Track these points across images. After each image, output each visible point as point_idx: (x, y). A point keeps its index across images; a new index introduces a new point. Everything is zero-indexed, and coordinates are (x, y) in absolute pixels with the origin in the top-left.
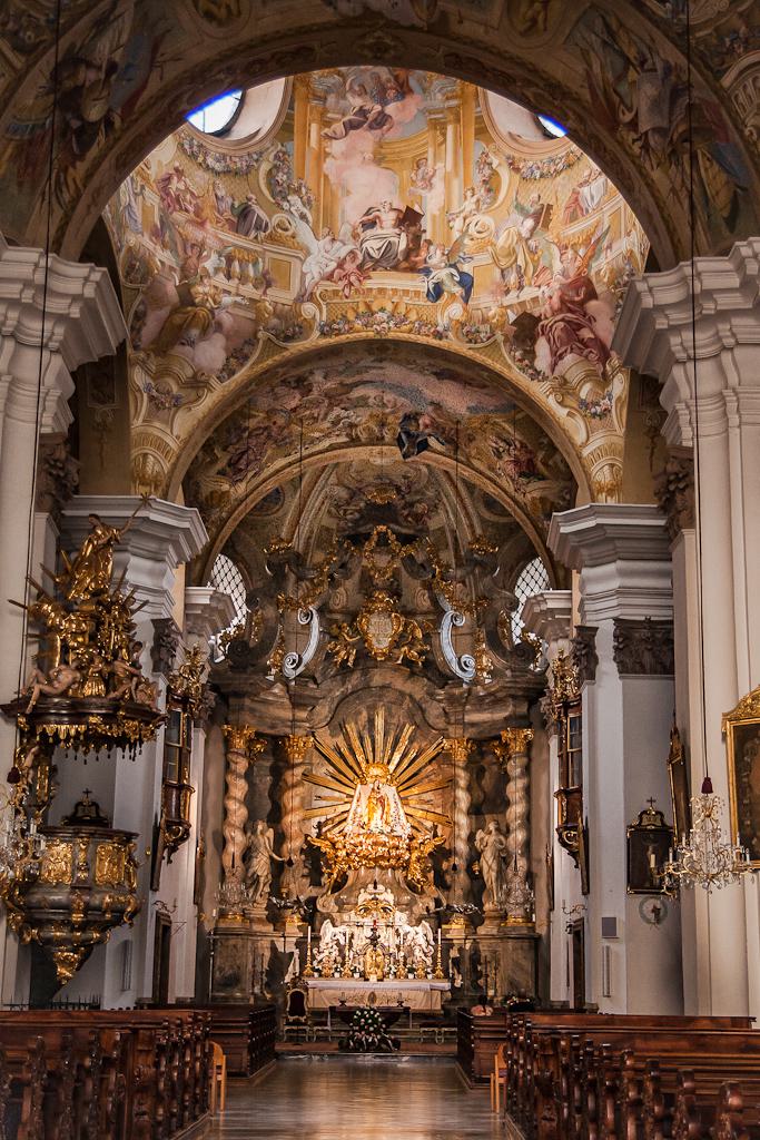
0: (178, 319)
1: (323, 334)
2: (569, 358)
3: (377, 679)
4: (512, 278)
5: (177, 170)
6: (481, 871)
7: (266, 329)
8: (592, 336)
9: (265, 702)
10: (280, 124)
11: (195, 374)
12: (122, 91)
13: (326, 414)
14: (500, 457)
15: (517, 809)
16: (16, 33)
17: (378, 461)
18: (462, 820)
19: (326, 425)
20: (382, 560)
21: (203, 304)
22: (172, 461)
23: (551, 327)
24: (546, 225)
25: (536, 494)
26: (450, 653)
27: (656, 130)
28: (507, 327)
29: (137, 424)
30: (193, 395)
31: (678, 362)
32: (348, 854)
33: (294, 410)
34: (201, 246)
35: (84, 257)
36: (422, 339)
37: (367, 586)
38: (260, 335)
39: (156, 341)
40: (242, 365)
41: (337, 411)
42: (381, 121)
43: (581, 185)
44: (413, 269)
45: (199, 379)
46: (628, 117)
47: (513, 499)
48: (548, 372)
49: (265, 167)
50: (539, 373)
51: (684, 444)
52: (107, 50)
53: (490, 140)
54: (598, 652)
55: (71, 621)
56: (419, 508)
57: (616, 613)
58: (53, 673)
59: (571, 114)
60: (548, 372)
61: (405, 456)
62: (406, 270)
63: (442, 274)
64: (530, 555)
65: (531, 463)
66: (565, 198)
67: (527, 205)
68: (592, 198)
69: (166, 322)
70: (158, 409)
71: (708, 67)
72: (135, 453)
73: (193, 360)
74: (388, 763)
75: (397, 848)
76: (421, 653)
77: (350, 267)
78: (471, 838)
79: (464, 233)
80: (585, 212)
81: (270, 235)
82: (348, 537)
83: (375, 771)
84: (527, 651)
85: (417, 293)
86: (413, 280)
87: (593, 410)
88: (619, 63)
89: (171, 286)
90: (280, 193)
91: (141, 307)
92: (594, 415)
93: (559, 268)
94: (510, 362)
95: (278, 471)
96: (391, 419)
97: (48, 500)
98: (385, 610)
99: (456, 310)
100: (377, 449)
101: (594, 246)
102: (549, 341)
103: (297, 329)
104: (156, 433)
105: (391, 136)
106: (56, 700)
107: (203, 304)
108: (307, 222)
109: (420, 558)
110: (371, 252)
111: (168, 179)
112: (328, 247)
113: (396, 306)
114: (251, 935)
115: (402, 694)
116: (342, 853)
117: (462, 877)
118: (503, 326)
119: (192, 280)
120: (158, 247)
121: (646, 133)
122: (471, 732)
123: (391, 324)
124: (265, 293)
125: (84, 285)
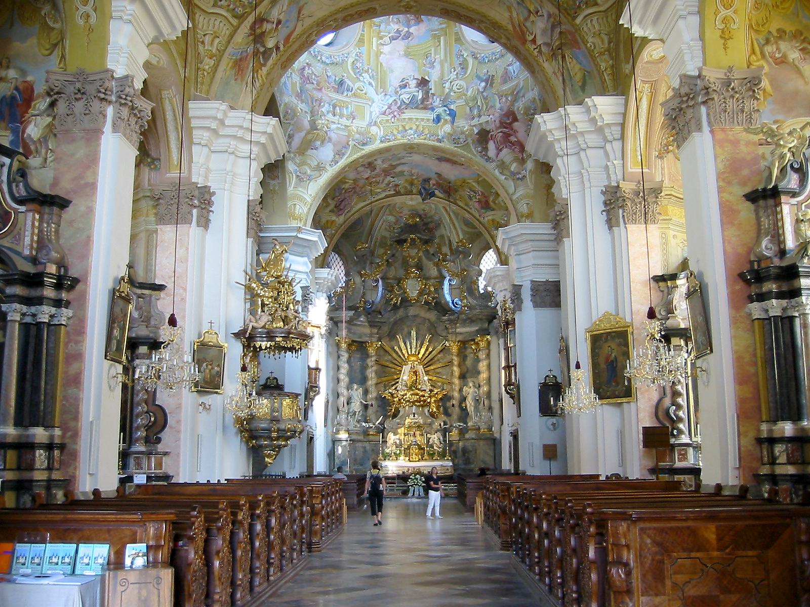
0: (309, 137)
1: (382, 142)
2: (505, 151)
3: (412, 311)
4: (476, 112)
5: (307, 64)
6: (466, 407)
7: (353, 140)
9: (356, 325)
11: (319, 163)
12: (284, 32)
13: (383, 180)
14: (470, 198)
15: (484, 376)
16: (234, 9)
17: (410, 203)
19: (383, 185)
20: (413, 252)
21: (321, 130)
22: (308, 207)
24: (491, 85)
25: (490, 218)
26: (448, 298)
27: (545, 44)
28: (474, 136)
29: (290, 189)
30: (318, 175)
31: (559, 156)
32: (399, 400)
33: (367, 179)
34: (320, 101)
35: (267, 113)
36: (431, 143)
37: (406, 265)
38: (350, 143)
41: (389, 178)
42: (408, 35)
43: (508, 66)
44: (425, 108)
46: (531, 38)
47: (478, 220)
48: (494, 158)
49: (350, 60)
50: (490, 158)
51: (563, 197)
52: (276, 15)
53: (462, 44)
54: (523, 297)
55: (265, 291)
56: (431, 225)
57: (530, 278)
58: (258, 317)
59: (503, 36)
60: (494, 158)
61: (423, 200)
62: (422, 109)
63: (440, 110)
64: (487, 248)
65: (487, 203)
66: (501, 72)
67: (482, 75)
68: (514, 72)
71: (568, 14)
72: (290, 204)
75: (424, 396)
76: (433, 298)
77: (394, 108)
78: (461, 390)
79: (451, 90)
80: (511, 79)
81: (354, 93)
82: (396, 241)
83: (413, 358)
84: (488, 296)
85: (428, 120)
86: (426, 113)
87: (517, 176)
88: (526, 13)
89: (306, 122)
90: (358, 72)
91: (292, 132)
92: (519, 178)
93: (499, 105)
95: (360, 209)
96: (416, 182)
97: (252, 232)
98: (414, 277)
99: (448, 128)
100: (409, 197)
101: (516, 95)
105: (412, 43)
106: (260, 330)
108: (372, 86)
109: (432, 251)
110: (404, 100)
111: (304, 69)
112: (383, 98)
113: (418, 126)
117: (457, 409)
118: (471, 135)
119: (316, 117)
120: (299, 102)
121: (540, 45)
122: (460, 338)
123: (416, 136)
124: (352, 122)
125: (267, 127)
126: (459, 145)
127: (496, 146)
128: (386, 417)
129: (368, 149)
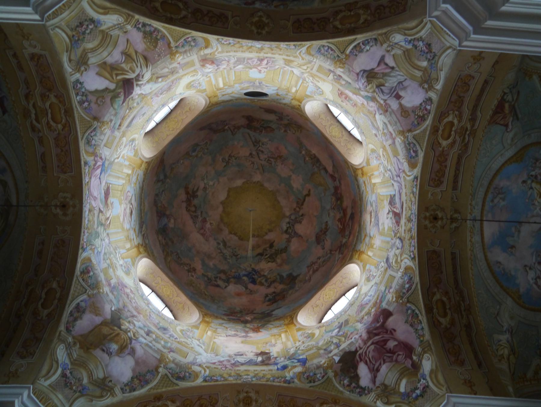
0: (105, 330)
2: (384, 368)
7: (165, 367)
8: (396, 343)
10: (192, 324)
11: (105, 378)
23: (366, 352)
30: (98, 392)
38: (160, 370)
39: (85, 336)
40: (142, 387)
45: (107, 383)
48: (371, 386)
50: (363, 389)
60: (371, 386)
69: (96, 327)
70: (66, 385)
73: (107, 366)
87: (414, 395)
94: (341, 389)
102: (366, 363)
103: (187, 374)
104: (56, 401)
107: (126, 331)
118: (330, 366)
126: (316, 383)
127: (369, 368)
129: (184, 384)
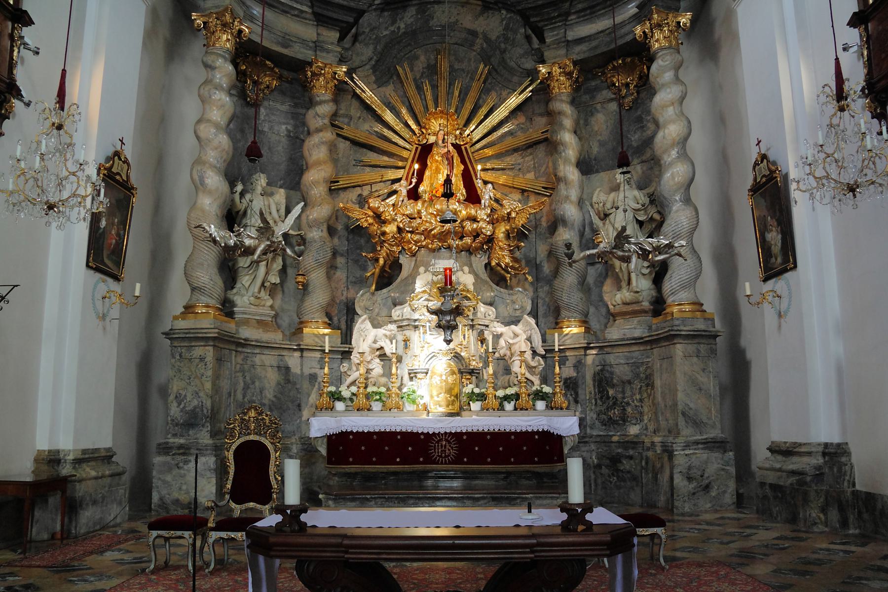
18: (572, 173)
32: (400, 230)
74: (458, 111)
114: (244, 345)
115: (474, 33)
116: (390, 229)
122: (580, 52)
128: (361, 282)
